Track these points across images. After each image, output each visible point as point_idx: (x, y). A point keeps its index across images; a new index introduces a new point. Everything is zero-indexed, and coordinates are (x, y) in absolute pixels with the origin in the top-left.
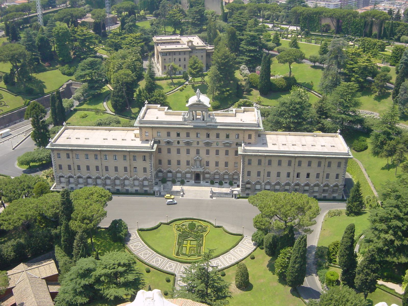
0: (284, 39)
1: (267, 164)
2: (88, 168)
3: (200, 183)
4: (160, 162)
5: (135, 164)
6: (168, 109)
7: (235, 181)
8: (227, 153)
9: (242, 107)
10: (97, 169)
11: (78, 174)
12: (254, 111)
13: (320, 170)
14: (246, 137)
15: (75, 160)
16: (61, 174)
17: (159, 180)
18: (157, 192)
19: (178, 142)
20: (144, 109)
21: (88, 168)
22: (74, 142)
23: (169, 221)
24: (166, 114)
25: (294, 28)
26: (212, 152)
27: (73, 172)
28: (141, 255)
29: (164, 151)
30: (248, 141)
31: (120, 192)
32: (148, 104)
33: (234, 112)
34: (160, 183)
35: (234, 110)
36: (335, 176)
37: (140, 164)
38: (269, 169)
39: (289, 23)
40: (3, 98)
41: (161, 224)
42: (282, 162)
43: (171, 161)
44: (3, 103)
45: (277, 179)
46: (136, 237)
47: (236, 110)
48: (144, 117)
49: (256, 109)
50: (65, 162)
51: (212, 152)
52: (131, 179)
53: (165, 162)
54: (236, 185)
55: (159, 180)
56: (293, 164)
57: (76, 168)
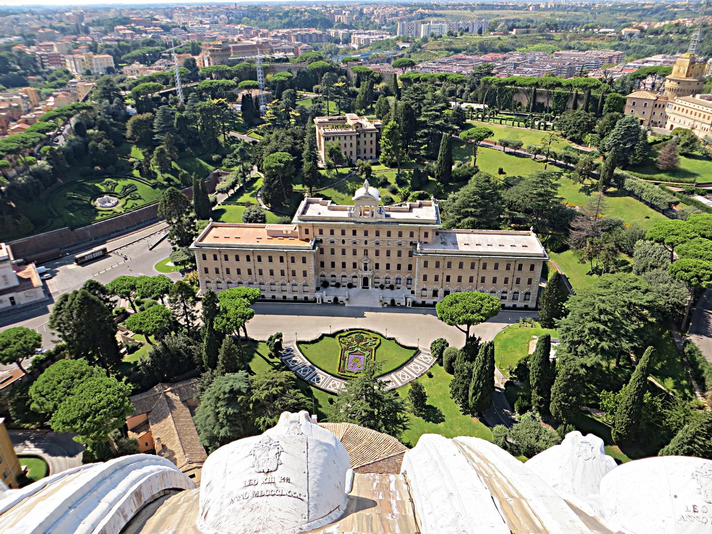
2: (239, 272)
4: (322, 264)
5: (293, 267)
10: (250, 272)
11: (228, 279)
12: (431, 205)
14: (422, 235)
15: (224, 262)
16: (207, 279)
19: (343, 242)
21: (239, 272)
23: (333, 331)
24: (330, 209)
25: (481, 106)
26: (383, 254)
27: (221, 277)
29: (327, 252)
30: (423, 239)
33: (408, 206)
34: (321, 288)
36: (527, 281)
37: (298, 266)
38: (448, 272)
39: (475, 100)
40: (136, 190)
41: (324, 335)
42: (464, 264)
44: (137, 196)
45: (458, 285)
48: (304, 213)
49: (433, 203)
50: (211, 263)
51: (383, 254)
53: (328, 264)
56: (476, 267)
57: (225, 271)
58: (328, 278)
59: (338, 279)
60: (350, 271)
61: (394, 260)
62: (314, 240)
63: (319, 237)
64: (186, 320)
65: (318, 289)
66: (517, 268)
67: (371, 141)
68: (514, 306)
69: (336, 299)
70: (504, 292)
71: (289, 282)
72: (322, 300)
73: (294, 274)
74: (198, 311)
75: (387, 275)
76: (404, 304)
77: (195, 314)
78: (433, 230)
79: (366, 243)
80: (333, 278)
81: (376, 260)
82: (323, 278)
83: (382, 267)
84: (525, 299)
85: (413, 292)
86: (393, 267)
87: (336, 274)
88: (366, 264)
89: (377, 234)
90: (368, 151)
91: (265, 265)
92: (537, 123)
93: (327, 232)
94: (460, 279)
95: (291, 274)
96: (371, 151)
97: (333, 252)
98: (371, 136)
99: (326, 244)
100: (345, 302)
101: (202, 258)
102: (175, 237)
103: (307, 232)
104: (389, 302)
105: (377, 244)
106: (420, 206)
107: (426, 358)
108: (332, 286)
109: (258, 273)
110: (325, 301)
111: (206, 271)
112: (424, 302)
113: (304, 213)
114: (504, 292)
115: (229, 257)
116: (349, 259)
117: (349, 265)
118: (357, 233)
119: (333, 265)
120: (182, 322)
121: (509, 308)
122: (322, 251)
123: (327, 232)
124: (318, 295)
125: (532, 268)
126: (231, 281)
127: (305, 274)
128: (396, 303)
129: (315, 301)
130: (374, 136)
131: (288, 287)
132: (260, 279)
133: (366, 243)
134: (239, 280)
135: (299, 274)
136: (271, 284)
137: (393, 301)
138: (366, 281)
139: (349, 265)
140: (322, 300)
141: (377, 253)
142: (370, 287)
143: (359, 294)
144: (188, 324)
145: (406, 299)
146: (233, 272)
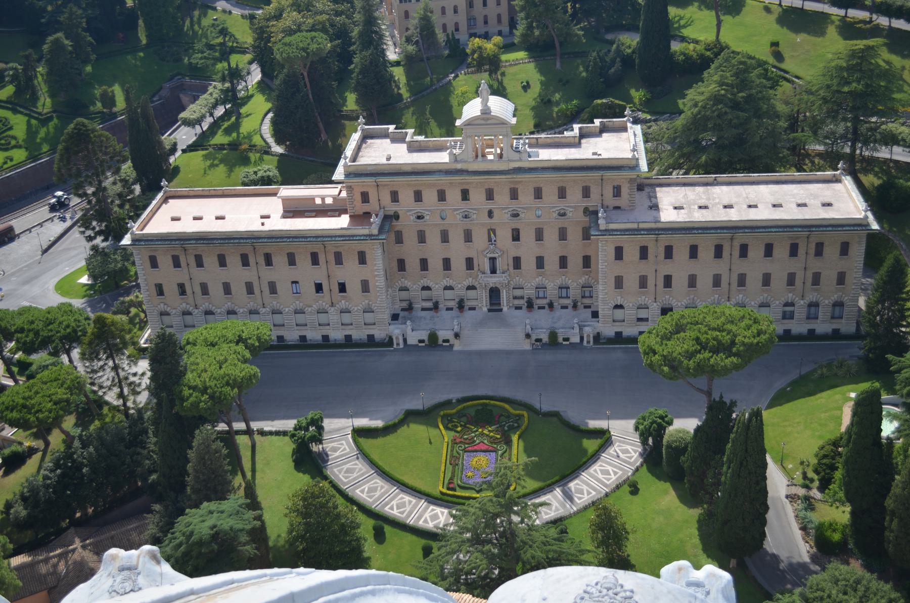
1: (662, 255)
3: (501, 310)
4: (402, 265)
6: (415, 134)
7: (587, 301)
8: (563, 235)
9: (595, 120)
11: (205, 306)
12: (624, 129)
13: (795, 265)
14: (609, 192)
15: (195, 270)
16: (162, 307)
17: (403, 310)
18: (397, 338)
20: (356, 137)
22: (187, 226)
26: (527, 236)
27: (191, 300)
28: (362, 491)
29: (410, 238)
31: (309, 342)
32: (366, 124)
34: (402, 314)
35: (576, 127)
40: (11, 128)
42: (700, 249)
43: (429, 261)
46: (348, 450)
47: (580, 129)
48: (354, 159)
50: (168, 275)
52: (333, 309)
53: (413, 264)
54: (589, 311)
55: (403, 310)
56: (726, 253)
57: (198, 290)
58: (415, 292)
59: (437, 292)
60: (460, 277)
61: (552, 248)
62: (381, 214)
63: (392, 208)
64: (121, 395)
65: (395, 317)
66: (812, 251)
68: (811, 332)
69: (433, 337)
70: (786, 305)
71: (332, 305)
72: (405, 340)
73: (342, 288)
74: (143, 374)
75: (538, 280)
76: (576, 339)
77: (135, 379)
78: (631, 181)
79: (490, 214)
80: (426, 293)
81: (513, 250)
82: (404, 294)
83: (529, 263)
84: (833, 317)
85: (595, 315)
86: (552, 263)
87: (431, 284)
88: (493, 260)
89: (514, 195)
91: (281, 272)
93: (406, 197)
94: (692, 282)
95: (336, 288)
97: (422, 238)
99: (407, 224)
100: (453, 340)
101: (148, 264)
102: (94, 223)
103: (365, 197)
104: (545, 338)
105: (516, 215)
106: (603, 130)
107: (626, 451)
108: (423, 309)
109: (266, 290)
110: (409, 342)
111: (160, 290)
112: (619, 334)
113: (354, 159)
114: (786, 305)
115: (206, 260)
116: (458, 251)
117: (458, 264)
118: (472, 195)
119: (424, 264)
120: (111, 397)
121: (800, 338)
122: (399, 239)
123: (406, 197)
124: (396, 331)
125: (845, 249)
126: (213, 309)
127: (365, 287)
128: (560, 340)
129: (389, 342)
131: (333, 316)
132: (272, 302)
133: (490, 214)
134: (229, 305)
135: (353, 287)
136: (297, 312)
137: (553, 335)
138: (494, 293)
139: (458, 264)
140: (405, 340)
141: (516, 236)
142: (505, 309)
143: (481, 324)
144: (125, 404)
145: (581, 329)
146: (216, 290)
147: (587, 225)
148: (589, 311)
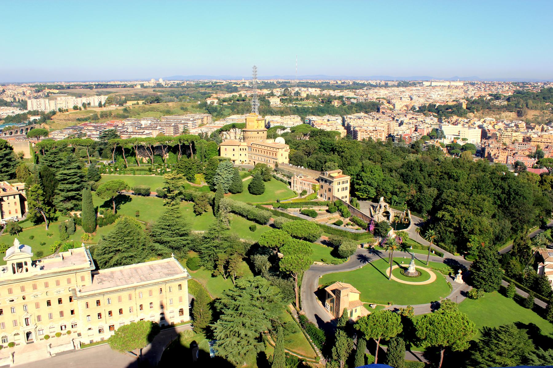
0: (103, 174)
7: (74, 329)
67: (15, 203)
90: (13, 212)
92: (159, 170)
96: (16, 212)
98: (14, 198)
112: (91, 342)
130: (17, 197)
147: (71, 296)
148: (76, 334)
